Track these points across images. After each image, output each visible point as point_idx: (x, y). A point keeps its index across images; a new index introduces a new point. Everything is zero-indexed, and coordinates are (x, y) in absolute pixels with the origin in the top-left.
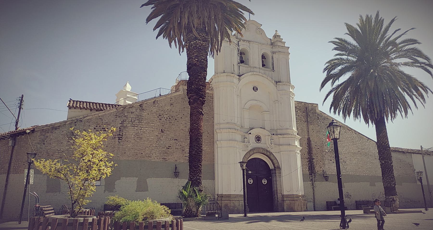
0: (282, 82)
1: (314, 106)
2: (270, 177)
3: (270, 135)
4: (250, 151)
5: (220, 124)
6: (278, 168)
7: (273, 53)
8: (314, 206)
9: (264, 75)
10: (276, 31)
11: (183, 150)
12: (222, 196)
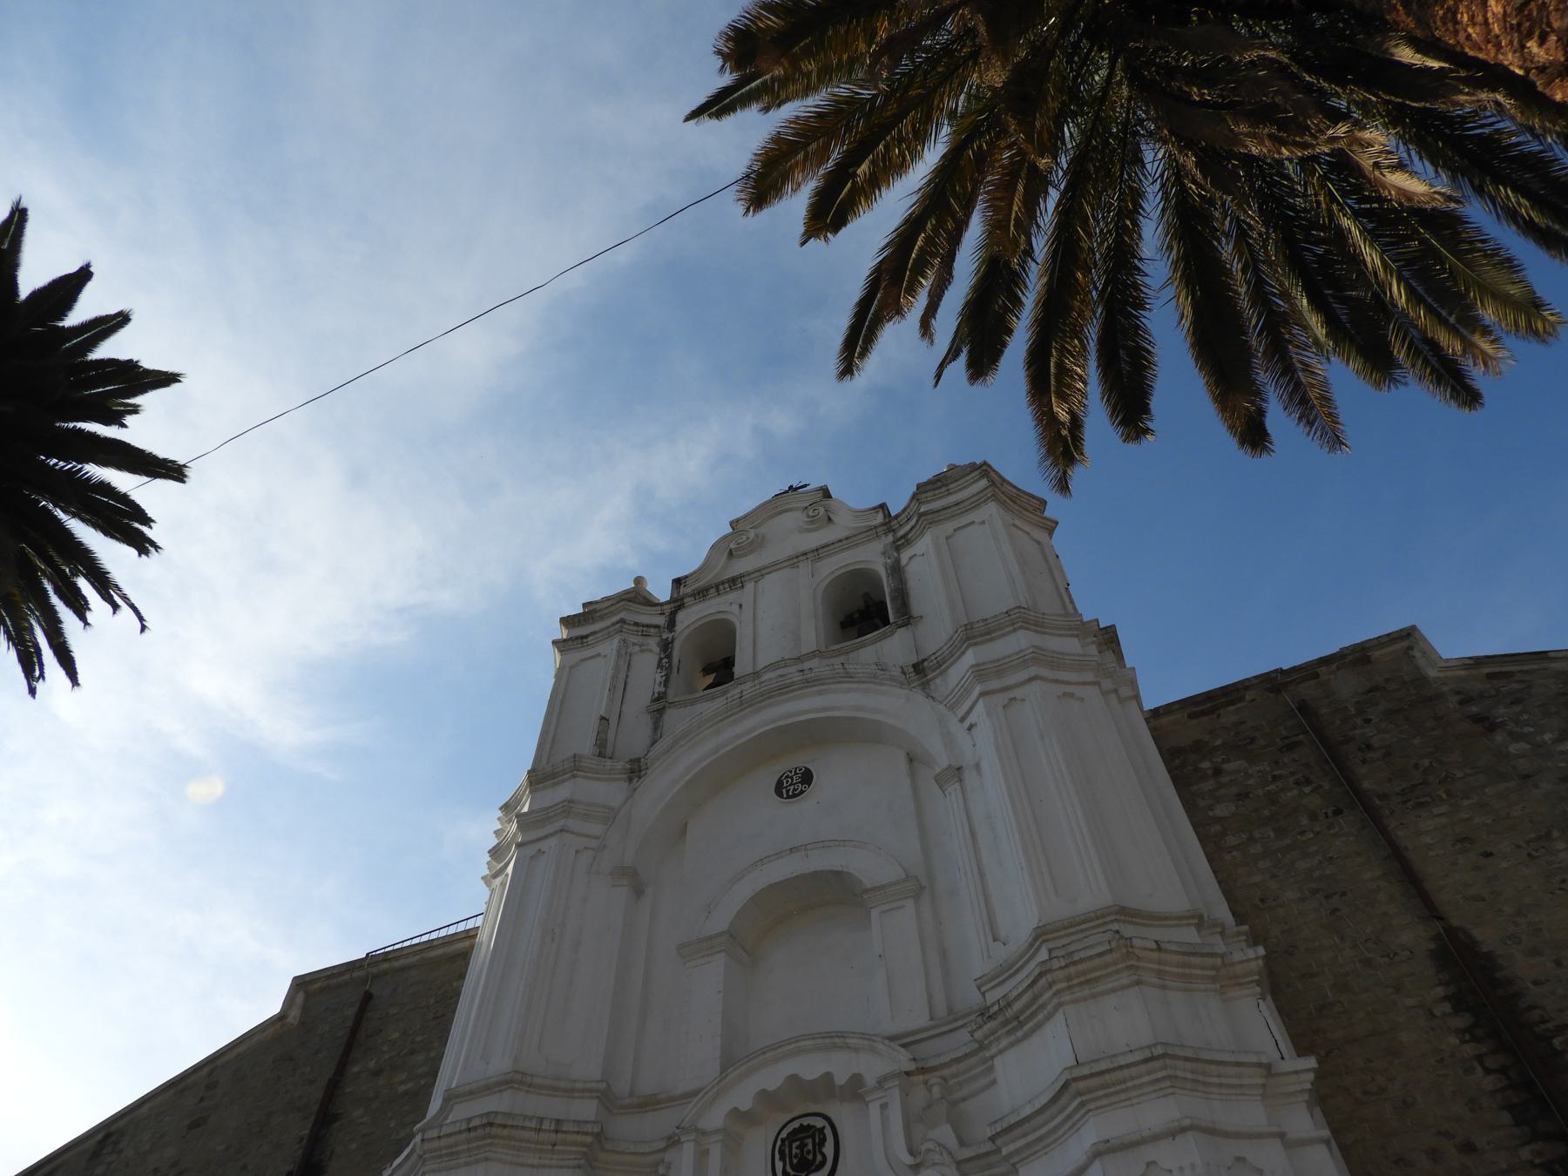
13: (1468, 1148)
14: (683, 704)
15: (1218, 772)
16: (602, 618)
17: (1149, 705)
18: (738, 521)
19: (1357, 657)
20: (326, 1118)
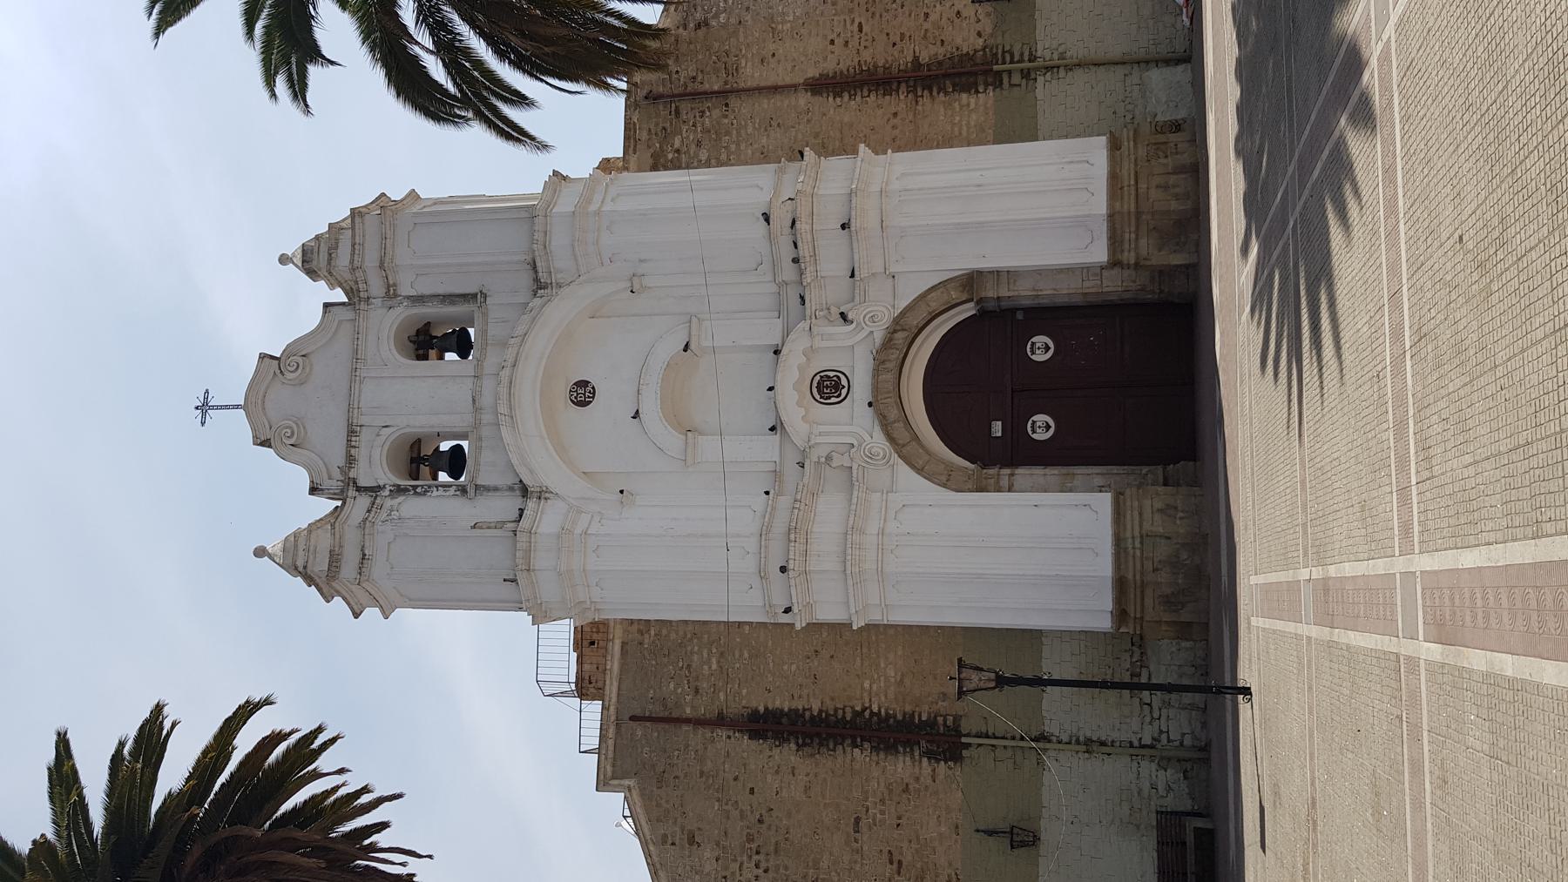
0: (535, 249)
2: (1020, 316)
3: (804, 325)
4: (891, 439)
5: (769, 606)
6: (971, 281)
9: (510, 354)
10: (284, 260)
11: (906, 789)
12: (1120, 614)
13: (895, 114)
15: (678, 151)
16: (341, 547)
18: (255, 437)
20: (720, 721)
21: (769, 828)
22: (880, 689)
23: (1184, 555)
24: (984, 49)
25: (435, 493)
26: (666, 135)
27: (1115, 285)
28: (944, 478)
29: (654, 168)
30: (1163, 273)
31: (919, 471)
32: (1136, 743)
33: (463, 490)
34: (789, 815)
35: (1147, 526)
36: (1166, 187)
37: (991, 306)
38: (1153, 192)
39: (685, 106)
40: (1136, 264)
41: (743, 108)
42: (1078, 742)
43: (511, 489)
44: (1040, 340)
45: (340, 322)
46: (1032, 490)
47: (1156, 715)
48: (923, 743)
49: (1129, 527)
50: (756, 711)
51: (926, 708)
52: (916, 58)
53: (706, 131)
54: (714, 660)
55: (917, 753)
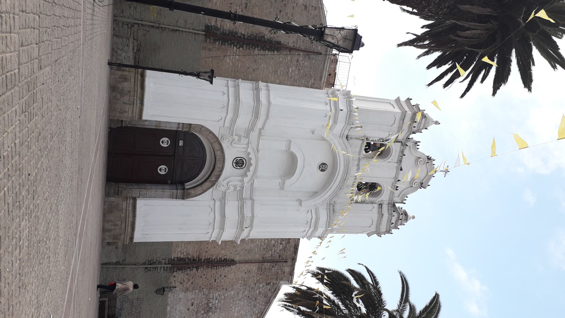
1: (289, 277)
2: (169, 182)
4: (220, 144)
7: (381, 205)
8: (109, 264)
12: (143, 76)
13: (206, 252)
14: (362, 145)
15: (281, 244)
17: (301, 239)
19: (292, 273)
21: (278, 8)
22: (233, 56)
23: (118, 96)
24: (174, 272)
25: (376, 139)
26: (284, 249)
27: (135, 191)
28: (203, 129)
29: (290, 239)
30: (118, 194)
31: (211, 132)
32: (140, 25)
33: (367, 139)
34: (270, 12)
35: (131, 107)
36: (115, 225)
37: (179, 186)
38: (120, 224)
39: (277, 258)
40: (127, 198)
41: (258, 257)
42: (162, 27)
43: (351, 138)
44: (163, 173)
45: (398, 197)
46: (171, 123)
47: (132, 35)
48: (219, 33)
49: (138, 108)
50: (278, 51)
51: (217, 46)
52: (197, 270)
53: (271, 250)
54: (290, 71)
55: (222, 30)
